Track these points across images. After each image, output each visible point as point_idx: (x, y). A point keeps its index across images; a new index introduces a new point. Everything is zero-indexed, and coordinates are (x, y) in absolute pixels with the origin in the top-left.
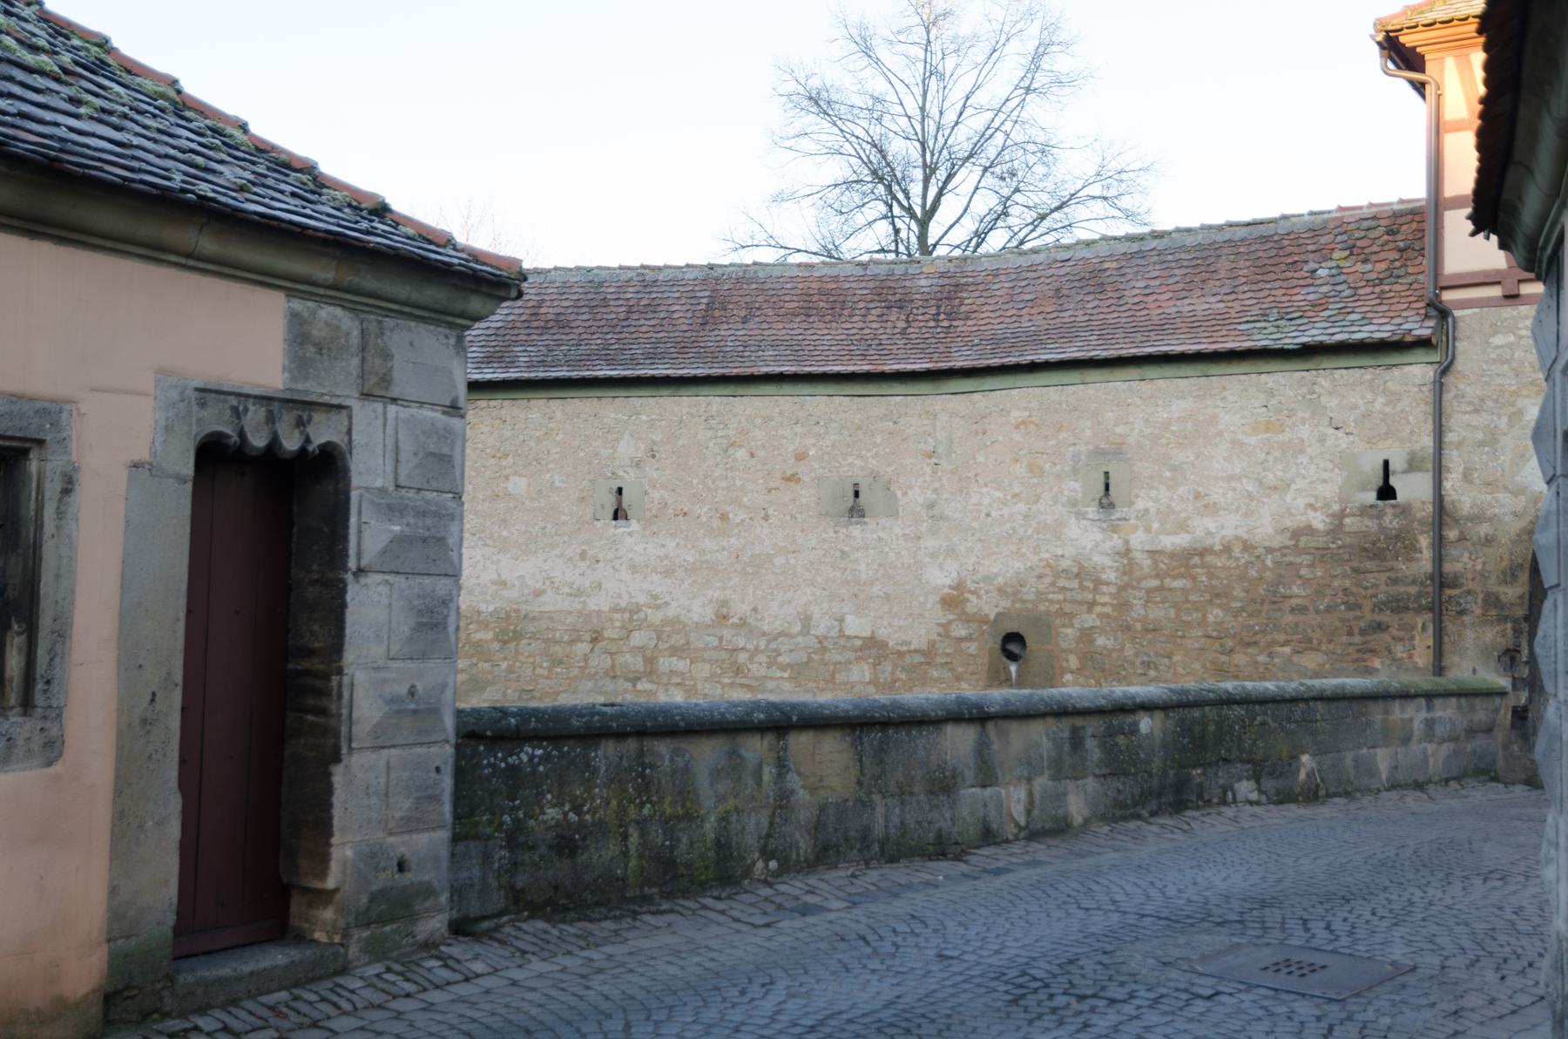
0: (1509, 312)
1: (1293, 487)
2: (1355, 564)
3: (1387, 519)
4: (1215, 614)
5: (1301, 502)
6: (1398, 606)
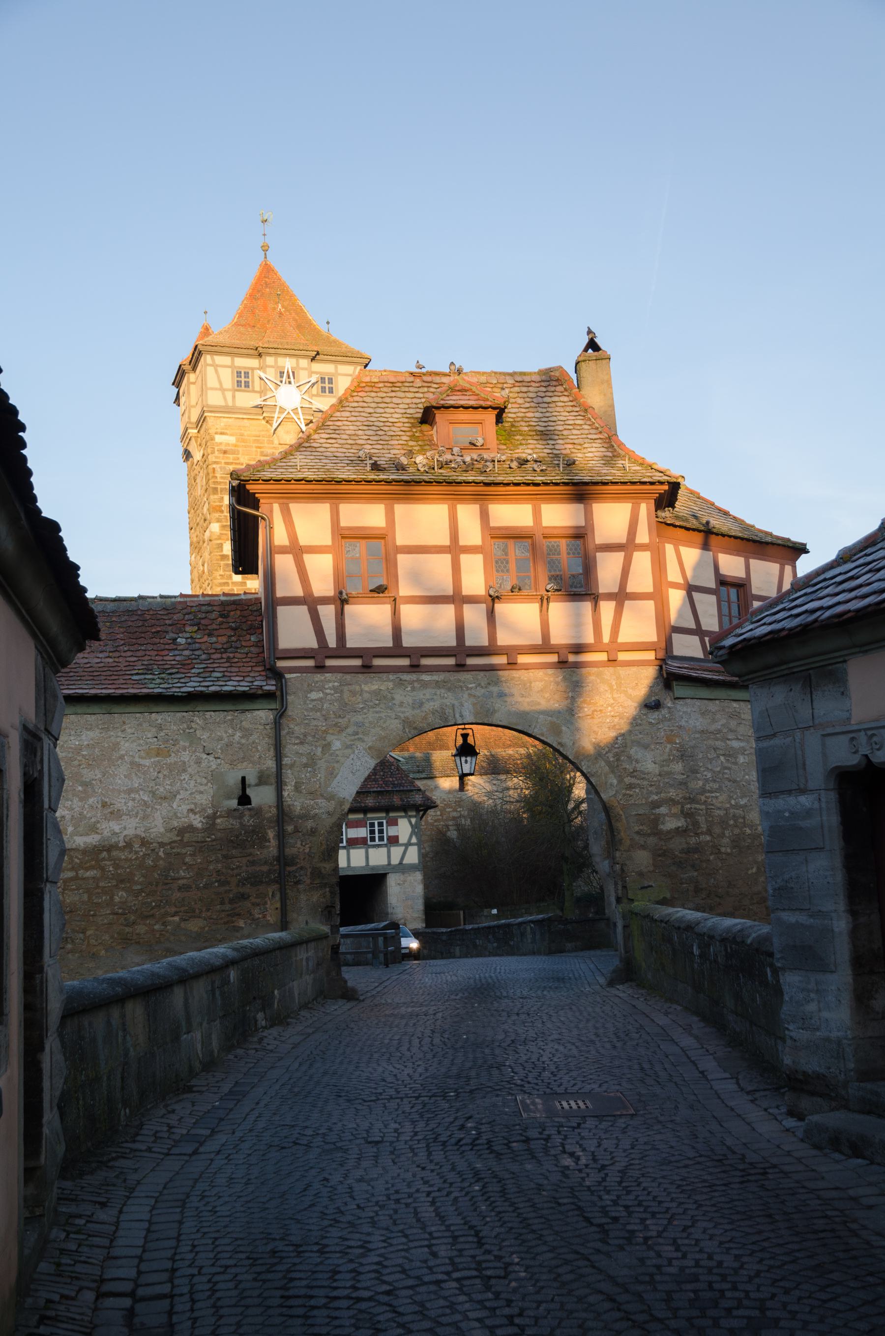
0: (318, 677)
1: (178, 797)
2: (224, 853)
3: (246, 819)
4: (120, 895)
5: (185, 808)
6: (255, 880)
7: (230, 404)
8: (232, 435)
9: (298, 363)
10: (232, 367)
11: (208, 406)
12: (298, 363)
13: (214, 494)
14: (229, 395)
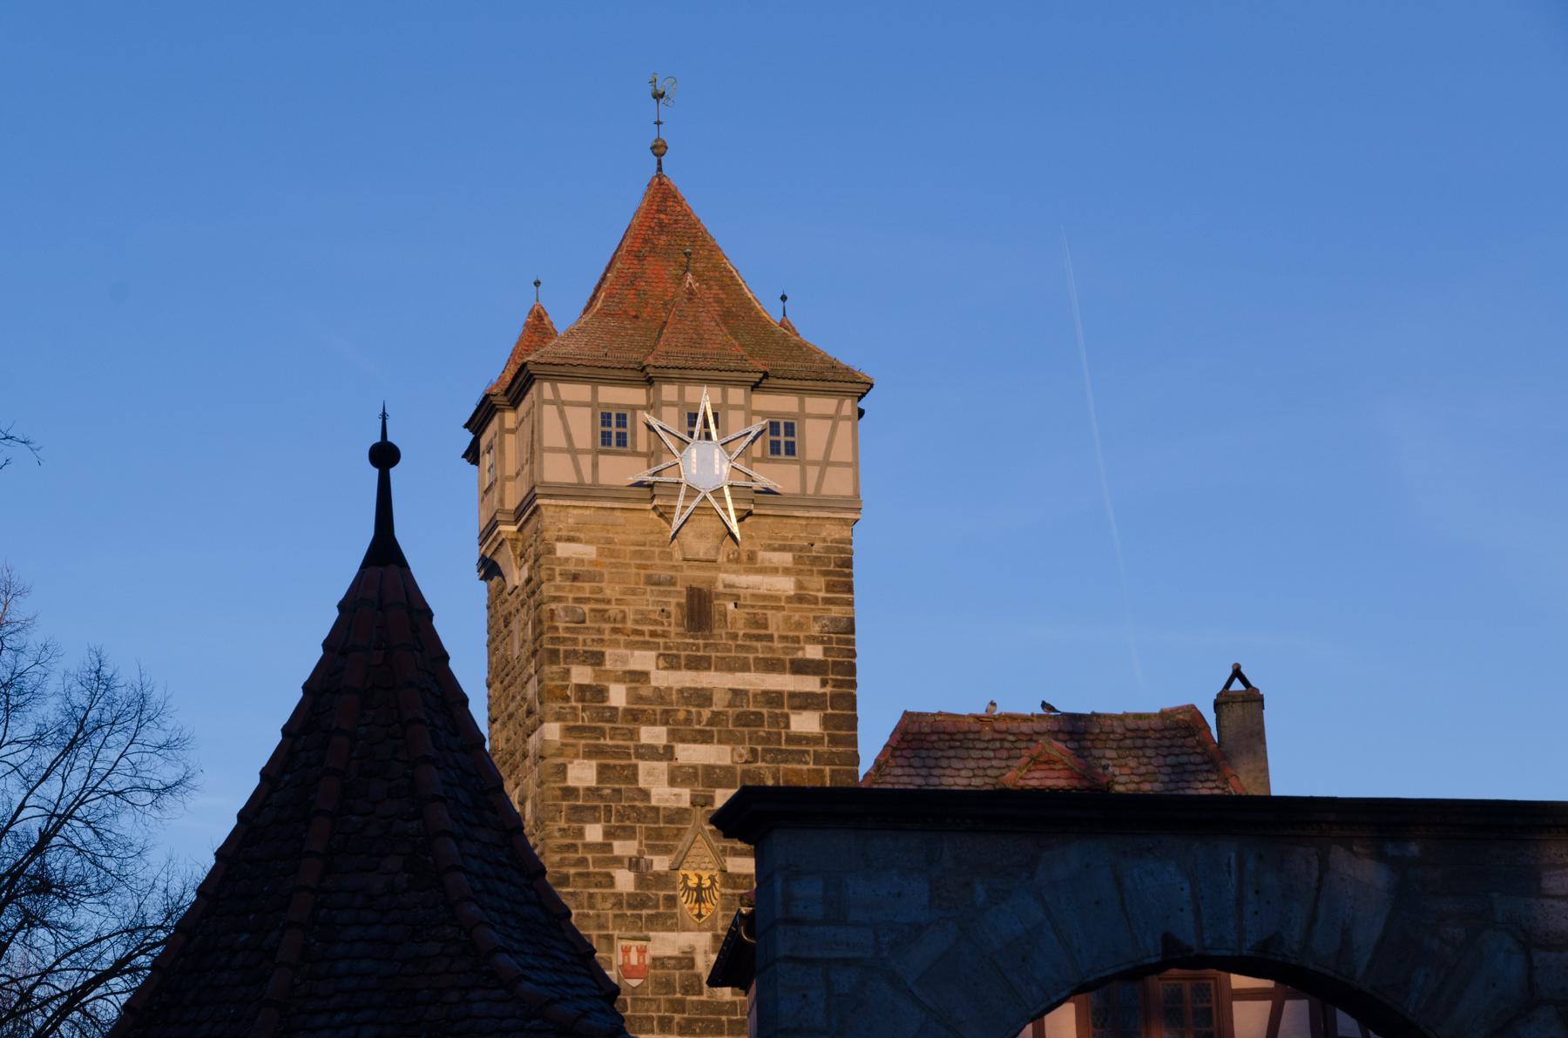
7: (588, 479)
8: (588, 542)
9: (725, 396)
10: (593, 404)
11: (544, 485)
12: (725, 396)
13: (552, 662)
14: (586, 462)
